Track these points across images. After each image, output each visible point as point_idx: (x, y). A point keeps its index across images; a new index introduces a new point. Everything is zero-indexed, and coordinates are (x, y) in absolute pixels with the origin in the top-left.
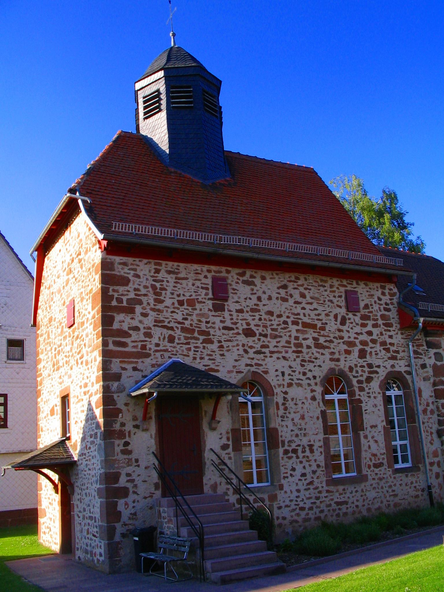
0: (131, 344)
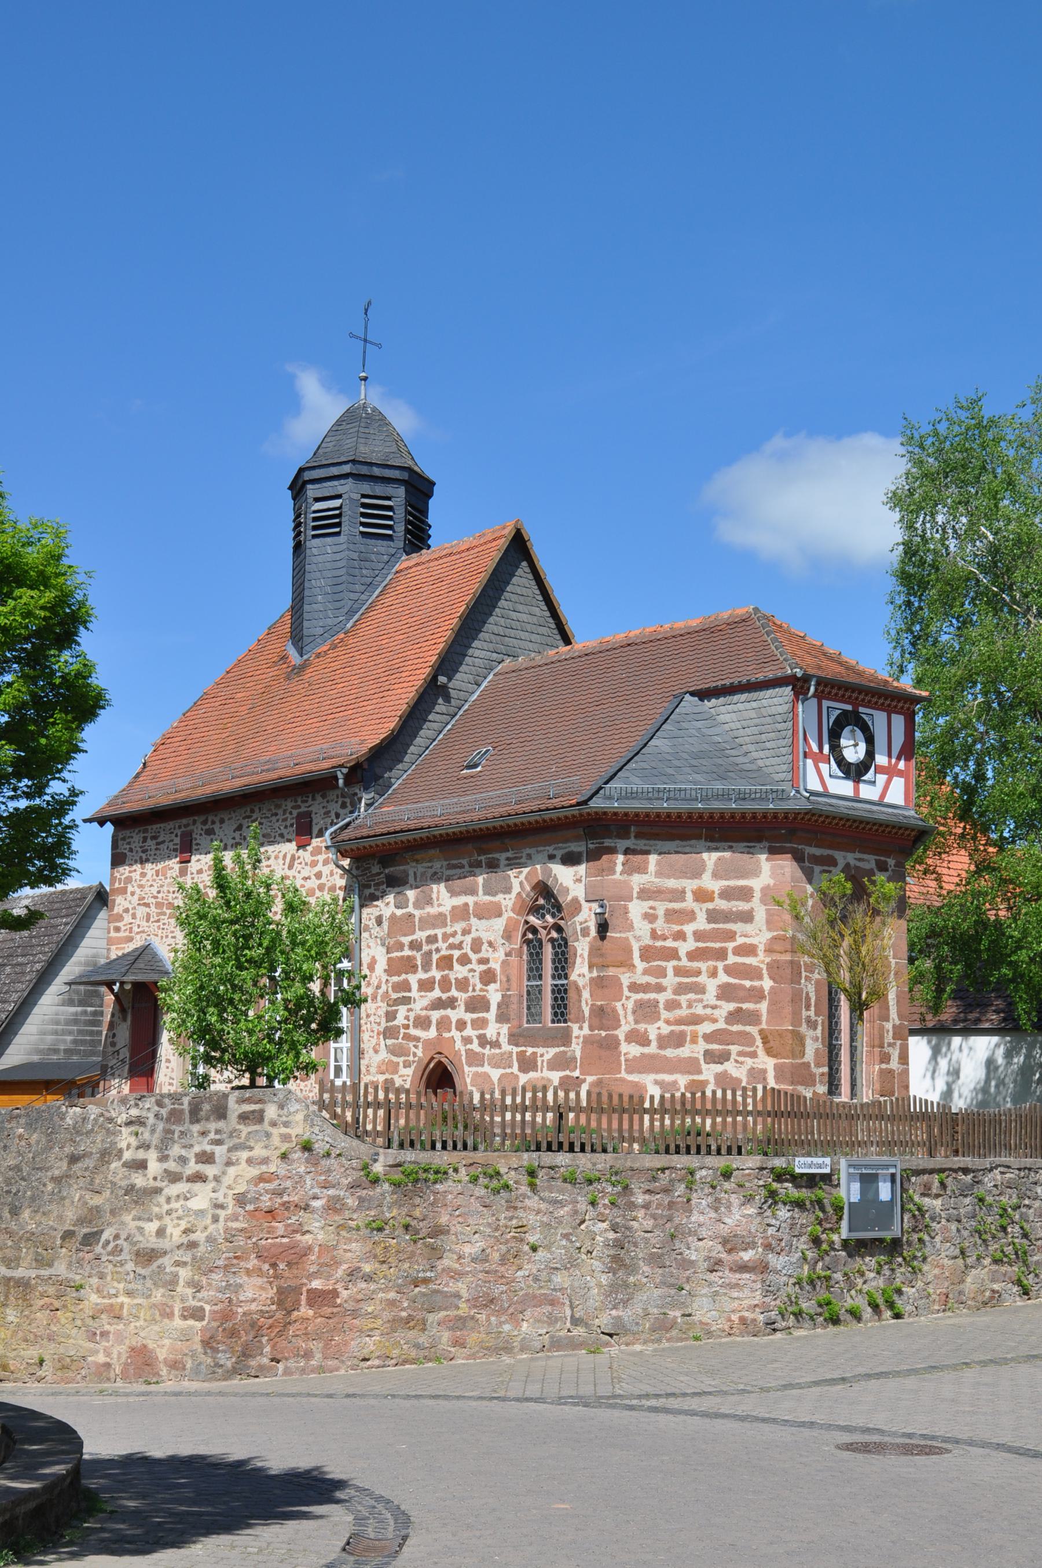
0: (123, 928)
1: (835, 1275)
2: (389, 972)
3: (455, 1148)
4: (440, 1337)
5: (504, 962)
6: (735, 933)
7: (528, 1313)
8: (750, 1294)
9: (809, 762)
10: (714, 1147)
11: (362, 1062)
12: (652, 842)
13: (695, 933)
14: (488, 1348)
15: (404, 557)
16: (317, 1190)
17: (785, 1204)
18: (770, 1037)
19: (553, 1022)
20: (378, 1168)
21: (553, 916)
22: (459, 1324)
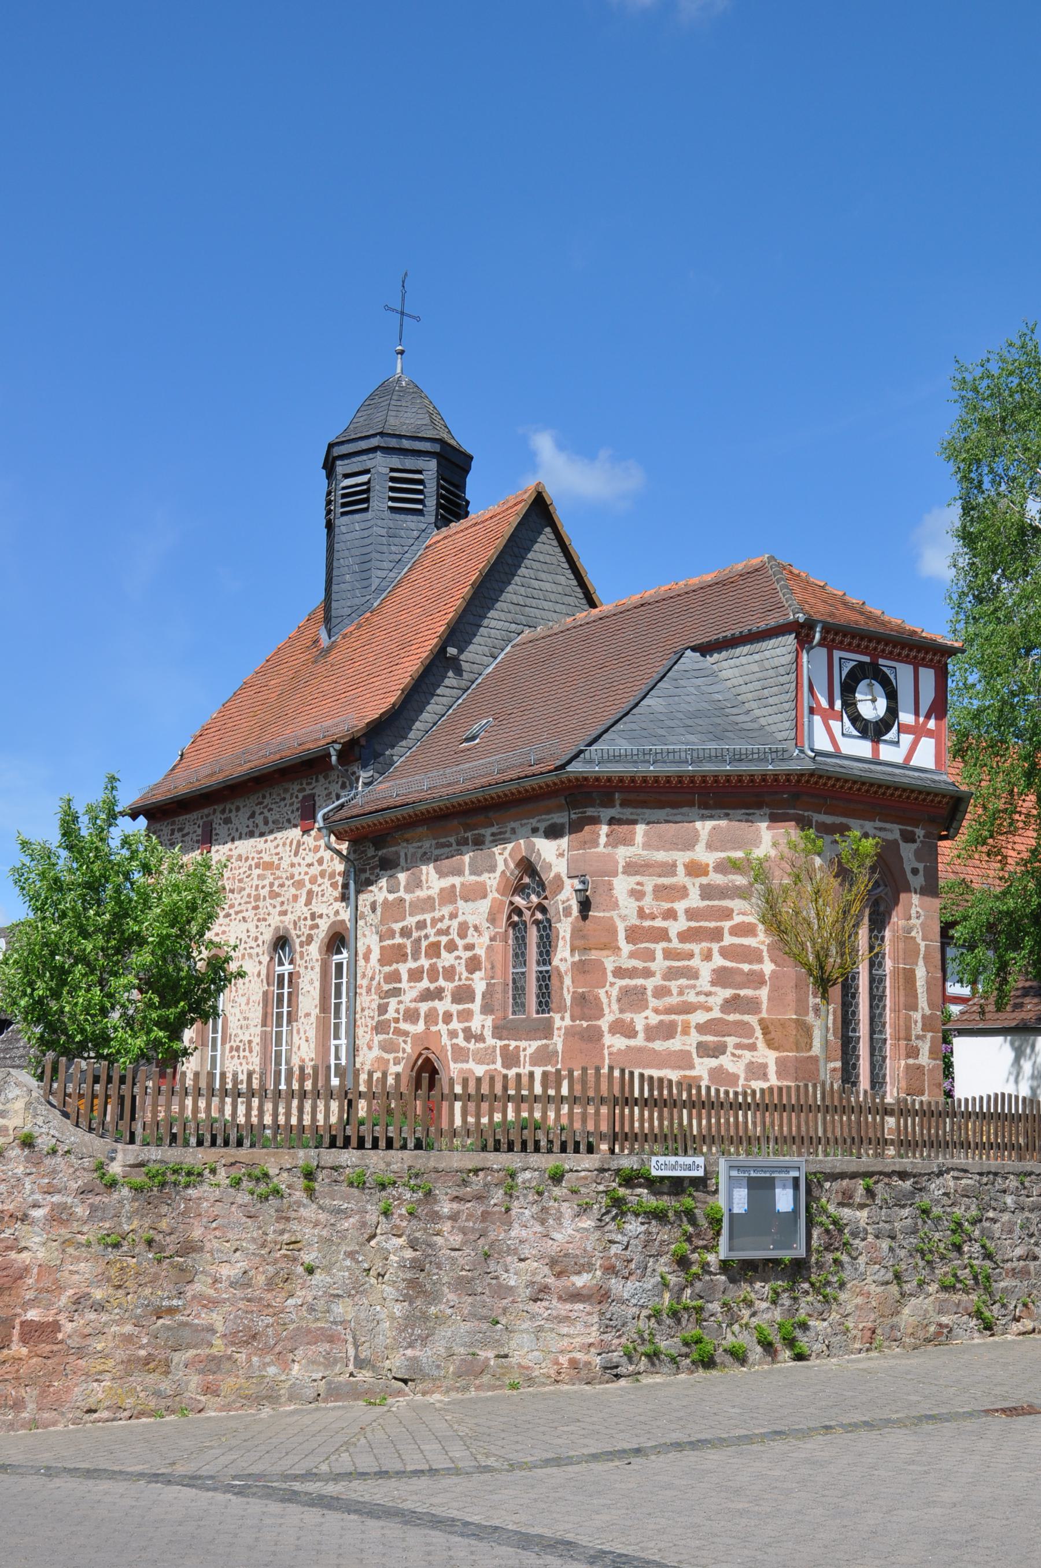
1: (710, 1306)
2: (382, 962)
3: (200, 1143)
4: (187, 1383)
5: (489, 948)
6: (732, 910)
7: (300, 1352)
8: (583, 1330)
9: (817, 719)
10: (543, 1143)
11: (357, 1059)
12: (639, 811)
13: (687, 911)
14: (247, 1397)
15: (436, 532)
16: (38, 1197)
17: (637, 1215)
18: (771, 1028)
19: (538, 1013)
20: (116, 1169)
21: (538, 895)
22: (213, 1366)
